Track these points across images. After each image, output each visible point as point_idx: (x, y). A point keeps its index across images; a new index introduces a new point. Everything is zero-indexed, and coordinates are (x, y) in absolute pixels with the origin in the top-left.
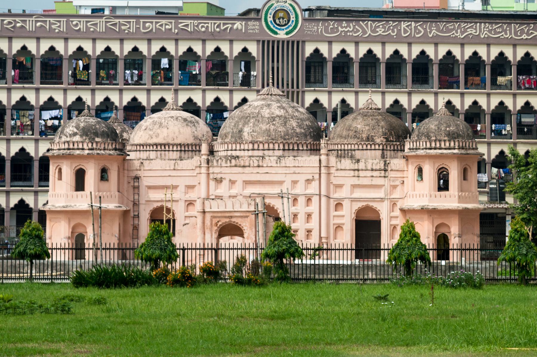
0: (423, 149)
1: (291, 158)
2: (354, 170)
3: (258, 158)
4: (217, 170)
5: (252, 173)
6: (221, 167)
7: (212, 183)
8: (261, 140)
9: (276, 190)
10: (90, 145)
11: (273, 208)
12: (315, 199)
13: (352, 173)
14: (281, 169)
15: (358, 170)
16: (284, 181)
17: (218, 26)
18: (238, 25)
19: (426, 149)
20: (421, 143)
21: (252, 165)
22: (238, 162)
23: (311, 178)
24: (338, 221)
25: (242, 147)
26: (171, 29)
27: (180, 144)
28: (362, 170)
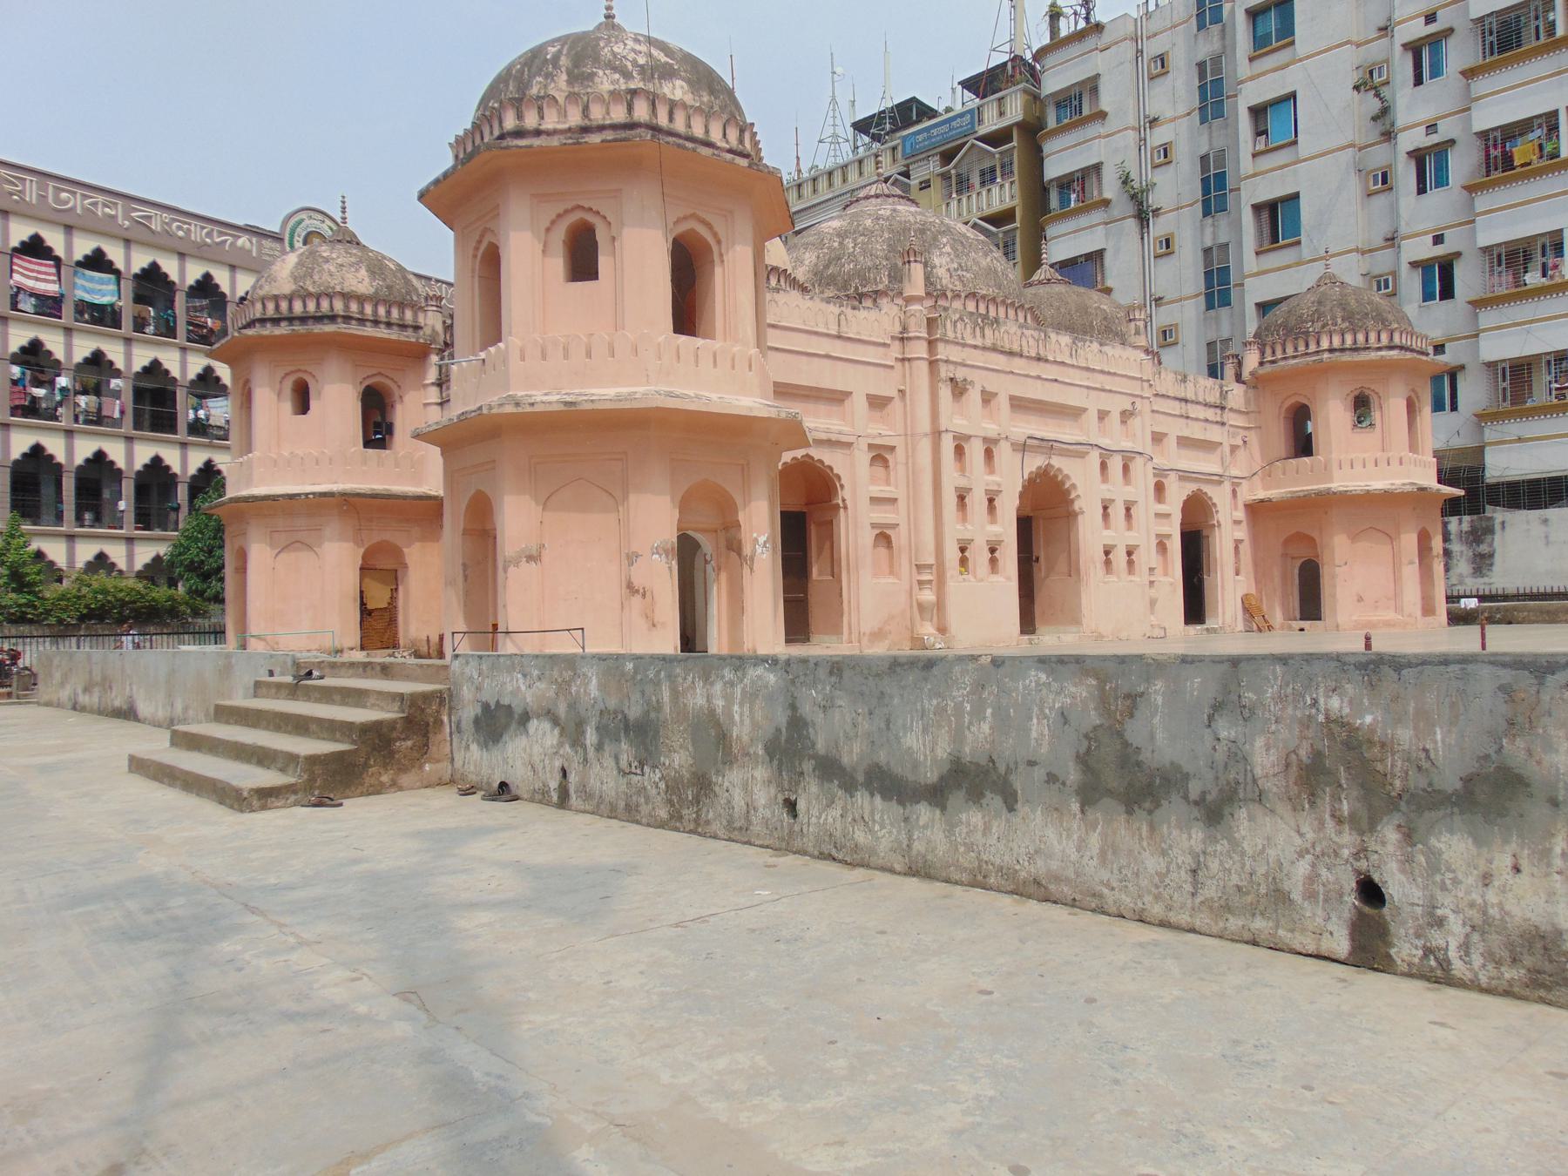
0: (1379, 349)
1: (1095, 346)
2: (1181, 400)
3: (1036, 334)
4: (954, 353)
5: (1027, 376)
6: (964, 345)
7: (945, 392)
9: (1065, 432)
10: (733, 135)
12: (1137, 465)
13: (1176, 407)
14: (1078, 372)
15: (1186, 401)
16: (1085, 410)
17: (209, 235)
18: (243, 241)
19: (1391, 348)
20: (1373, 337)
21: (1025, 349)
22: (990, 337)
23: (1129, 407)
24: (1165, 530)
26: (114, 217)
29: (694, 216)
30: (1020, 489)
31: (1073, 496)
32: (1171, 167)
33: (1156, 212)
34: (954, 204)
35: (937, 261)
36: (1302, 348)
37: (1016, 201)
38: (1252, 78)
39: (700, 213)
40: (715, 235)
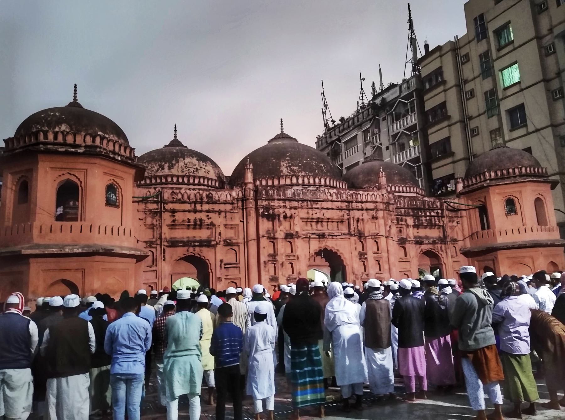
0: (515, 177)
6: (274, 200)
8: (303, 174)
10: (89, 140)
11: (336, 253)
12: (383, 241)
19: (521, 175)
25: (282, 182)
27: (204, 178)
28: (420, 209)
29: (70, 174)
30: (308, 257)
31: (342, 258)
32: (475, 98)
33: (471, 118)
34: (395, 125)
35: (282, 163)
36: (478, 180)
37: (416, 121)
38: (499, 58)
39: (72, 173)
40: (79, 179)
